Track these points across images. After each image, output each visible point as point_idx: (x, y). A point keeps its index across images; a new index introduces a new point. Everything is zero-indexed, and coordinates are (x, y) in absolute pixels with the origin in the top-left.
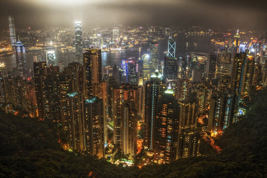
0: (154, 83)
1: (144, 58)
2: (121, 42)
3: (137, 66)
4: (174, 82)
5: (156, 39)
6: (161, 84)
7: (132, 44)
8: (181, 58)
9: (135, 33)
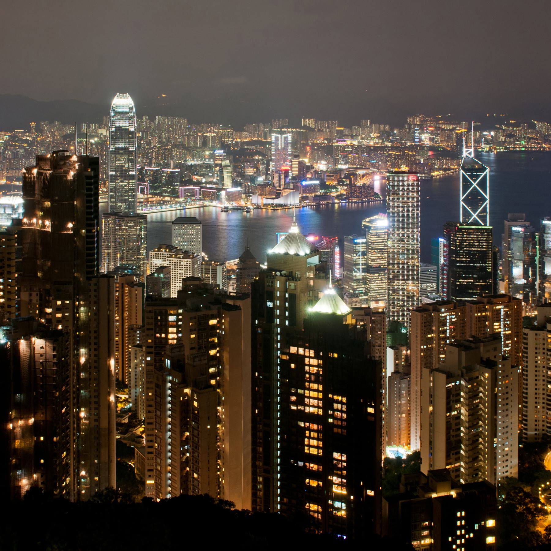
1: (369, 228)
2: (301, 176)
5: (439, 169)
7: (346, 185)
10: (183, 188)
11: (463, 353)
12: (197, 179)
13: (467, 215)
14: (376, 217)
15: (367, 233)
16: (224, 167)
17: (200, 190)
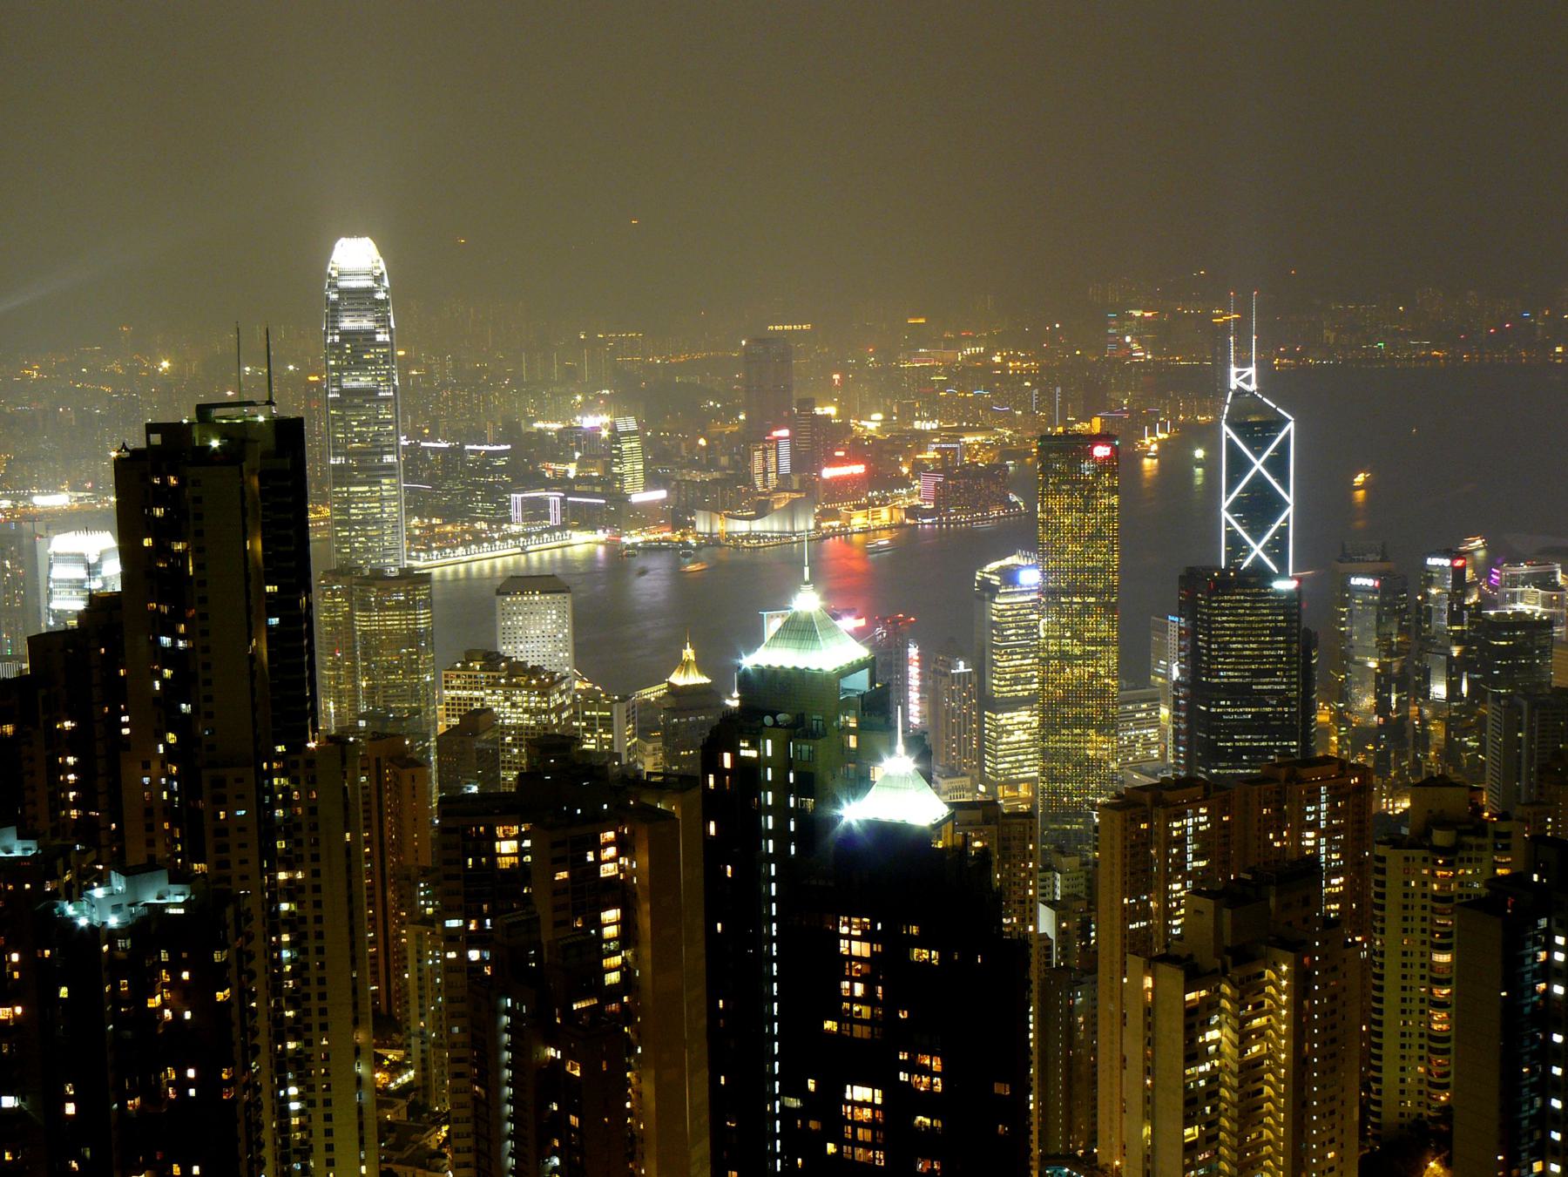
0: (776, 724)
3: (914, 670)
4: (1198, 791)
6: (853, 742)
8: (1370, 582)
9: (963, 375)
10: (520, 496)
11: (1227, 913)
12: (554, 471)
13: (1237, 546)
14: (1009, 561)
15: (987, 603)
16: (624, 434)
17: (563, 500)
